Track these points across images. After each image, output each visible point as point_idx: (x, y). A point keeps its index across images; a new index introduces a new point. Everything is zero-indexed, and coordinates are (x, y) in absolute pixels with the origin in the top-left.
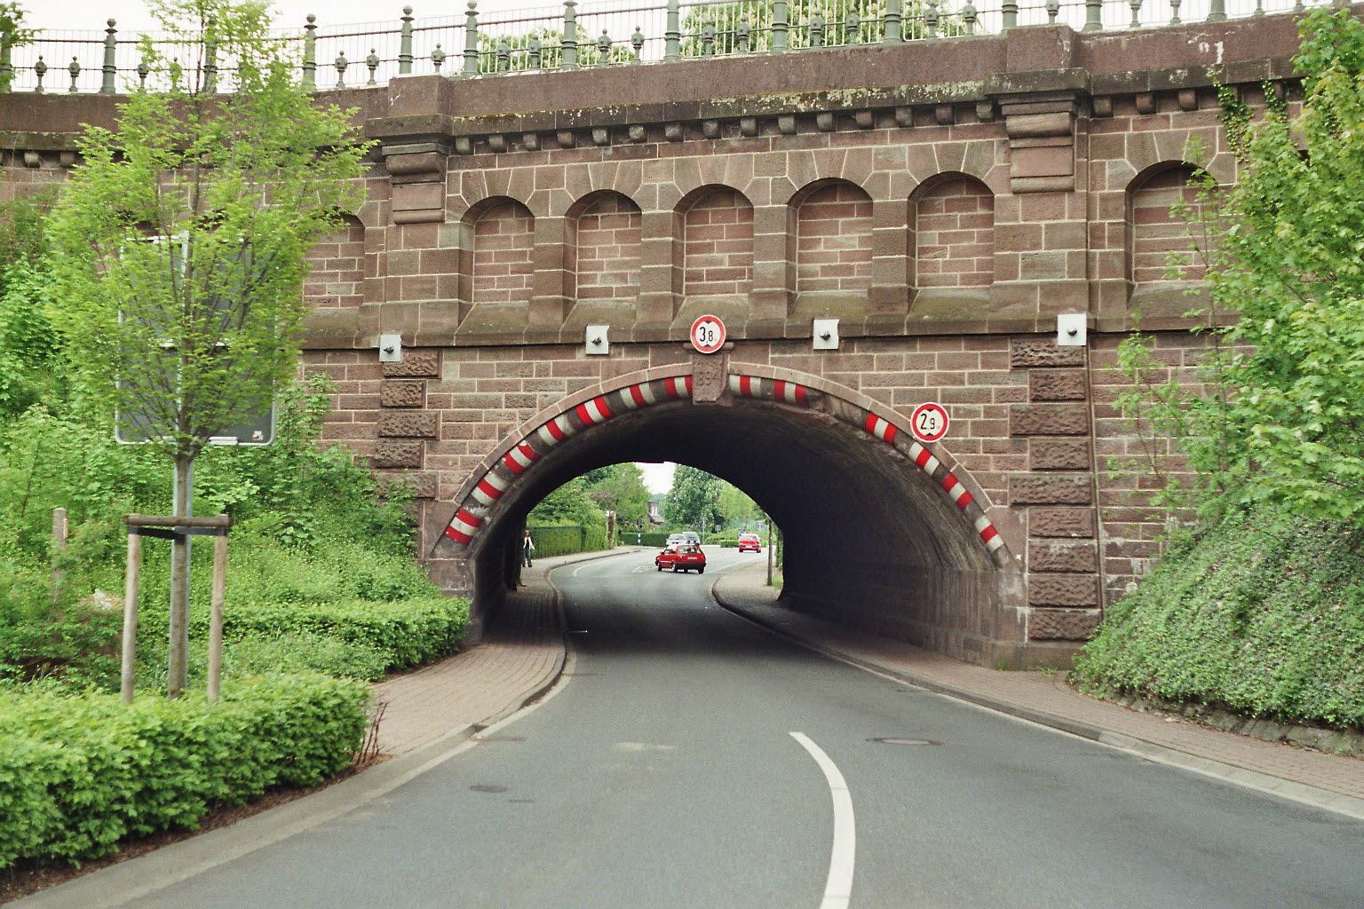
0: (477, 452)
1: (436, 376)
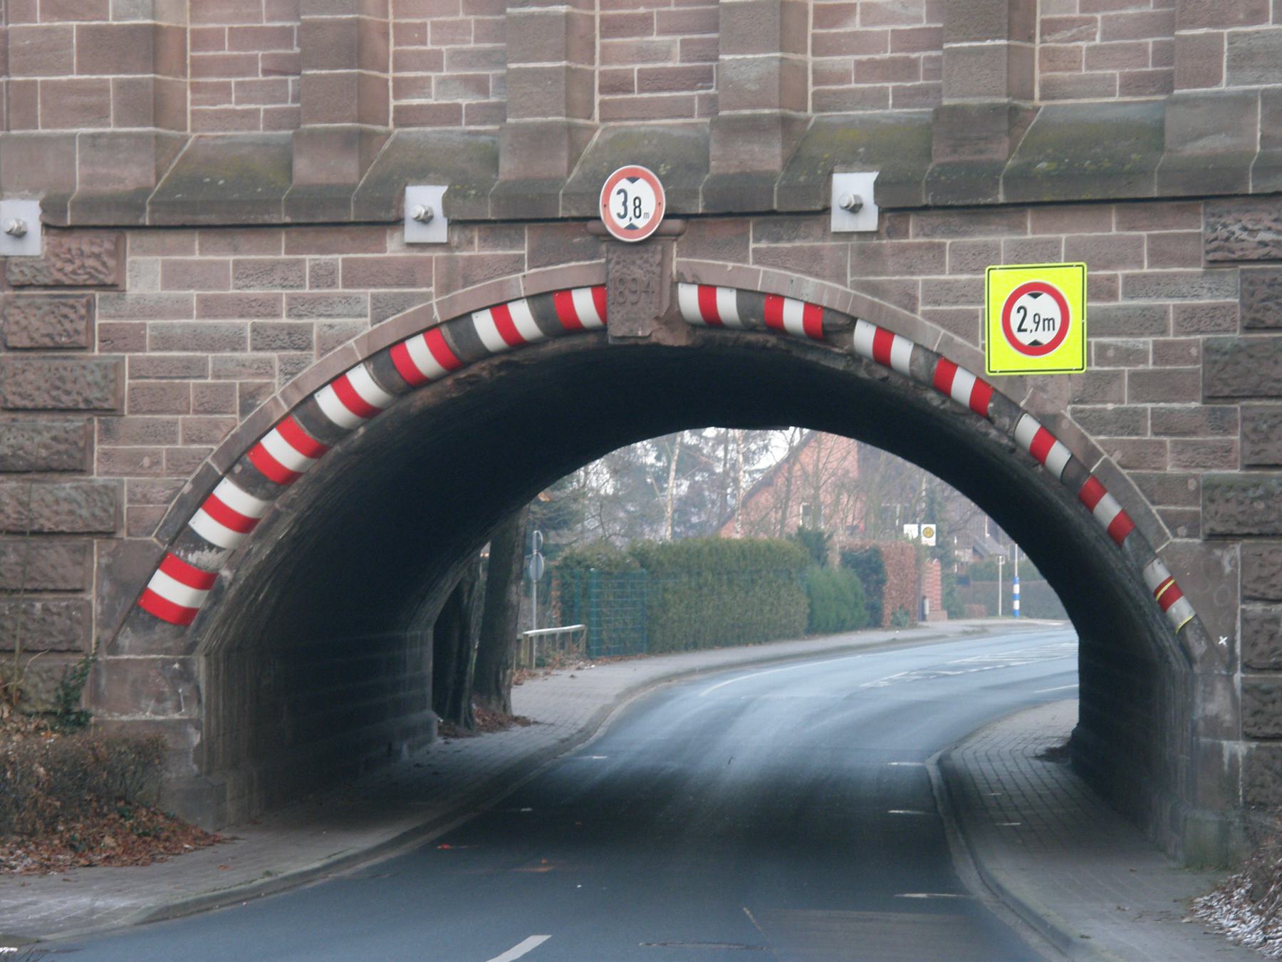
0: (200, 440)
1: (113, 286)
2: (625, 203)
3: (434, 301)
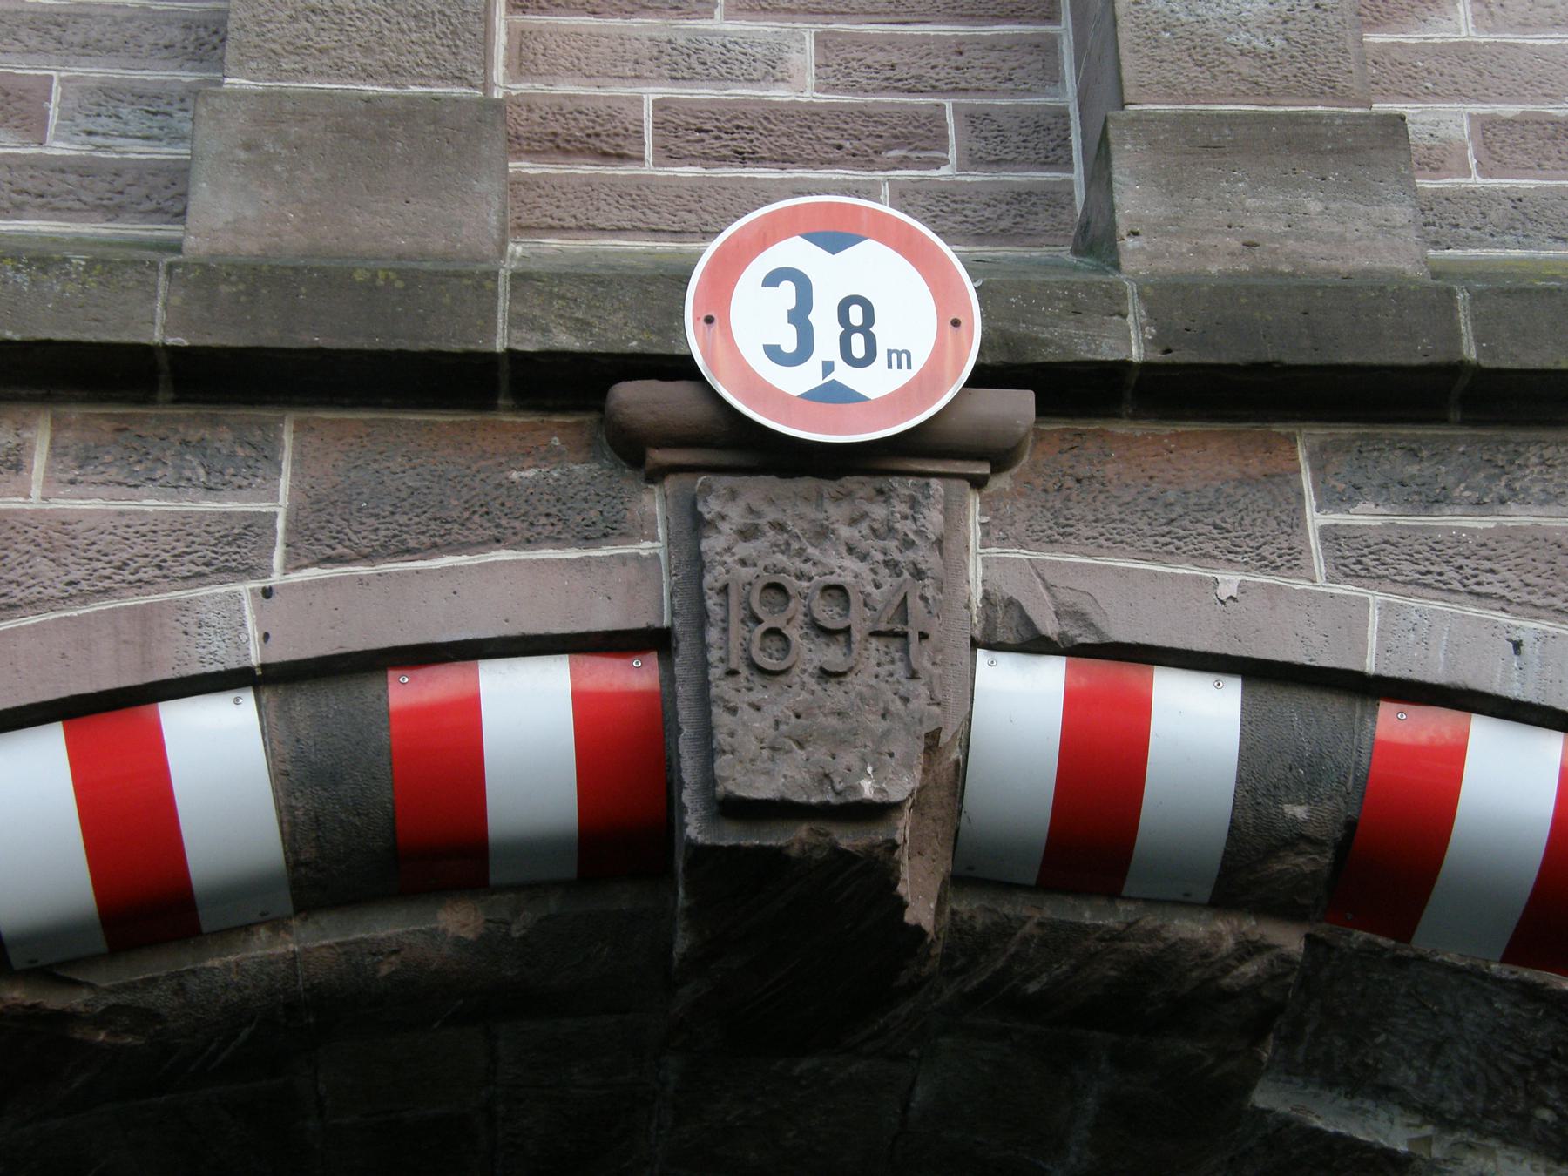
2: (800, 317)
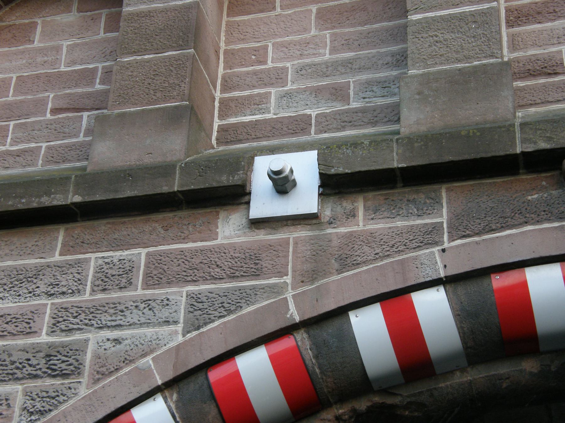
3: (289, 295)
